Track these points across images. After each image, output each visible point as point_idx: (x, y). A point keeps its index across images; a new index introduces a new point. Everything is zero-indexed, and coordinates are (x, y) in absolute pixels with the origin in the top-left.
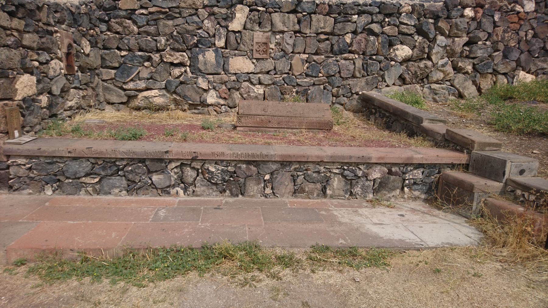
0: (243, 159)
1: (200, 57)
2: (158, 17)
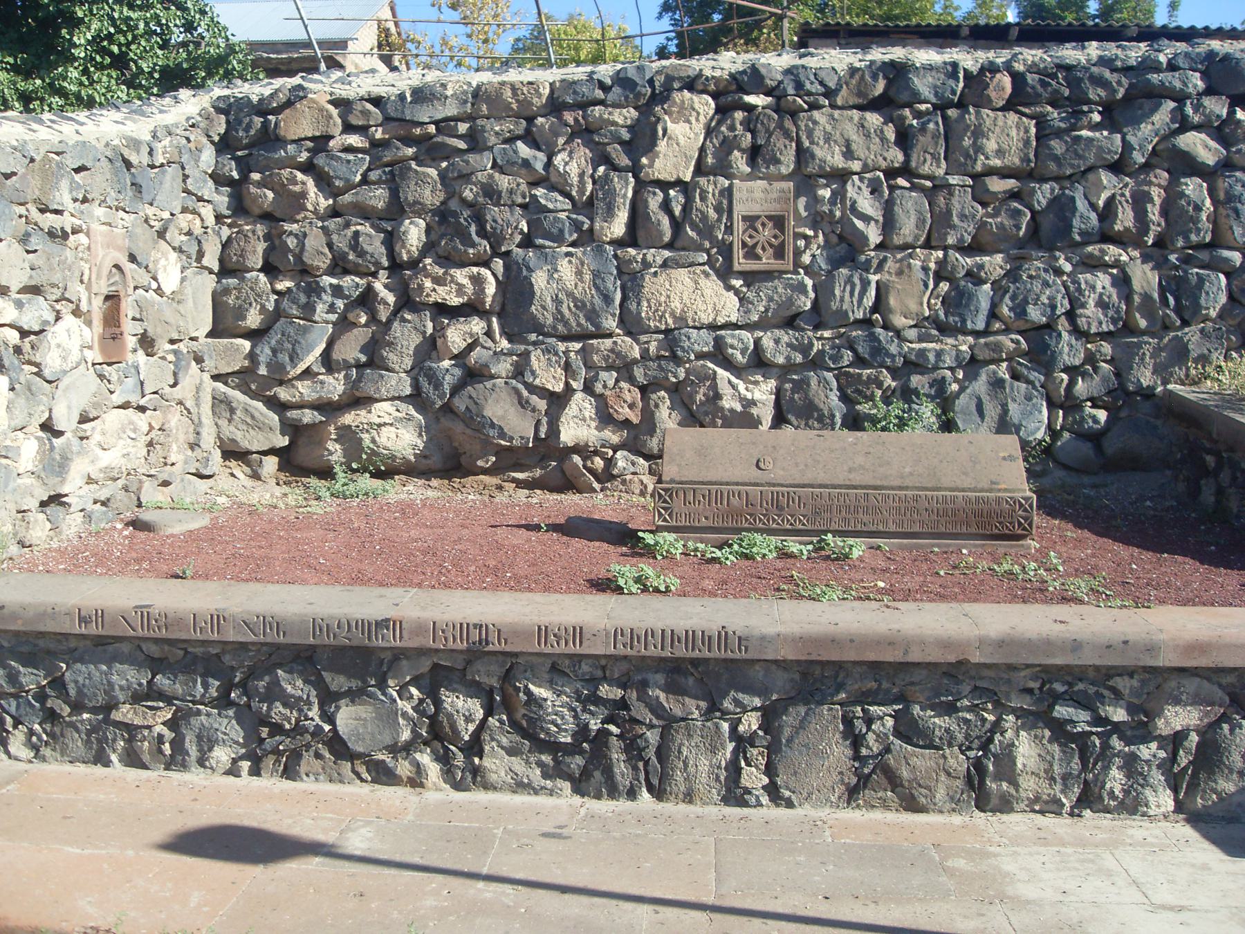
0: (652, 651)
1: (540, 280)
2: (400, 154)
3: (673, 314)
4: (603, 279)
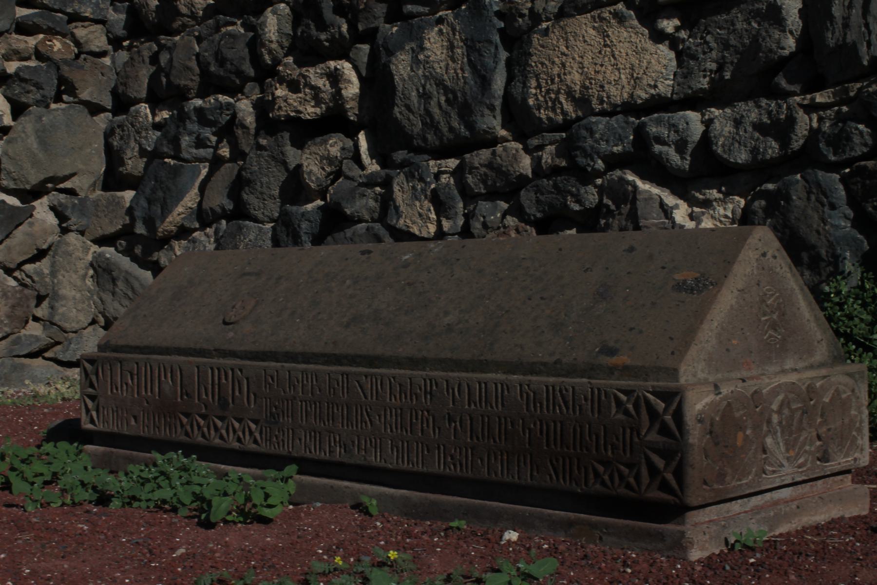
1: (401, 66)
3: (570, 94)
4: (479, 51)
